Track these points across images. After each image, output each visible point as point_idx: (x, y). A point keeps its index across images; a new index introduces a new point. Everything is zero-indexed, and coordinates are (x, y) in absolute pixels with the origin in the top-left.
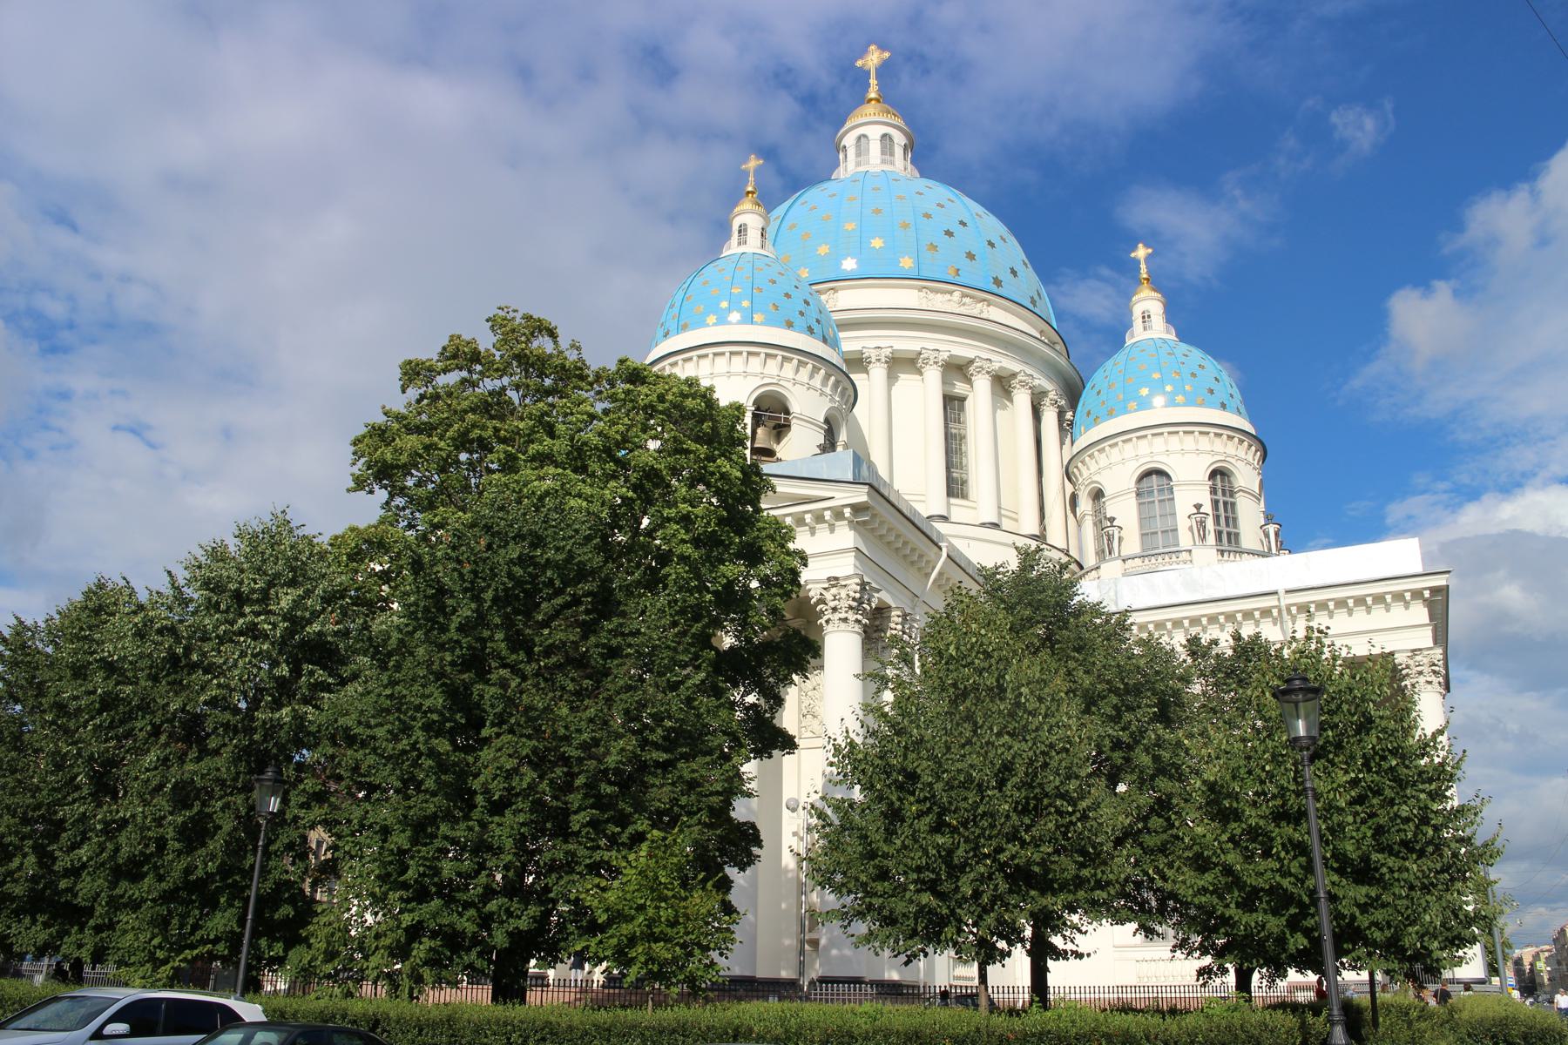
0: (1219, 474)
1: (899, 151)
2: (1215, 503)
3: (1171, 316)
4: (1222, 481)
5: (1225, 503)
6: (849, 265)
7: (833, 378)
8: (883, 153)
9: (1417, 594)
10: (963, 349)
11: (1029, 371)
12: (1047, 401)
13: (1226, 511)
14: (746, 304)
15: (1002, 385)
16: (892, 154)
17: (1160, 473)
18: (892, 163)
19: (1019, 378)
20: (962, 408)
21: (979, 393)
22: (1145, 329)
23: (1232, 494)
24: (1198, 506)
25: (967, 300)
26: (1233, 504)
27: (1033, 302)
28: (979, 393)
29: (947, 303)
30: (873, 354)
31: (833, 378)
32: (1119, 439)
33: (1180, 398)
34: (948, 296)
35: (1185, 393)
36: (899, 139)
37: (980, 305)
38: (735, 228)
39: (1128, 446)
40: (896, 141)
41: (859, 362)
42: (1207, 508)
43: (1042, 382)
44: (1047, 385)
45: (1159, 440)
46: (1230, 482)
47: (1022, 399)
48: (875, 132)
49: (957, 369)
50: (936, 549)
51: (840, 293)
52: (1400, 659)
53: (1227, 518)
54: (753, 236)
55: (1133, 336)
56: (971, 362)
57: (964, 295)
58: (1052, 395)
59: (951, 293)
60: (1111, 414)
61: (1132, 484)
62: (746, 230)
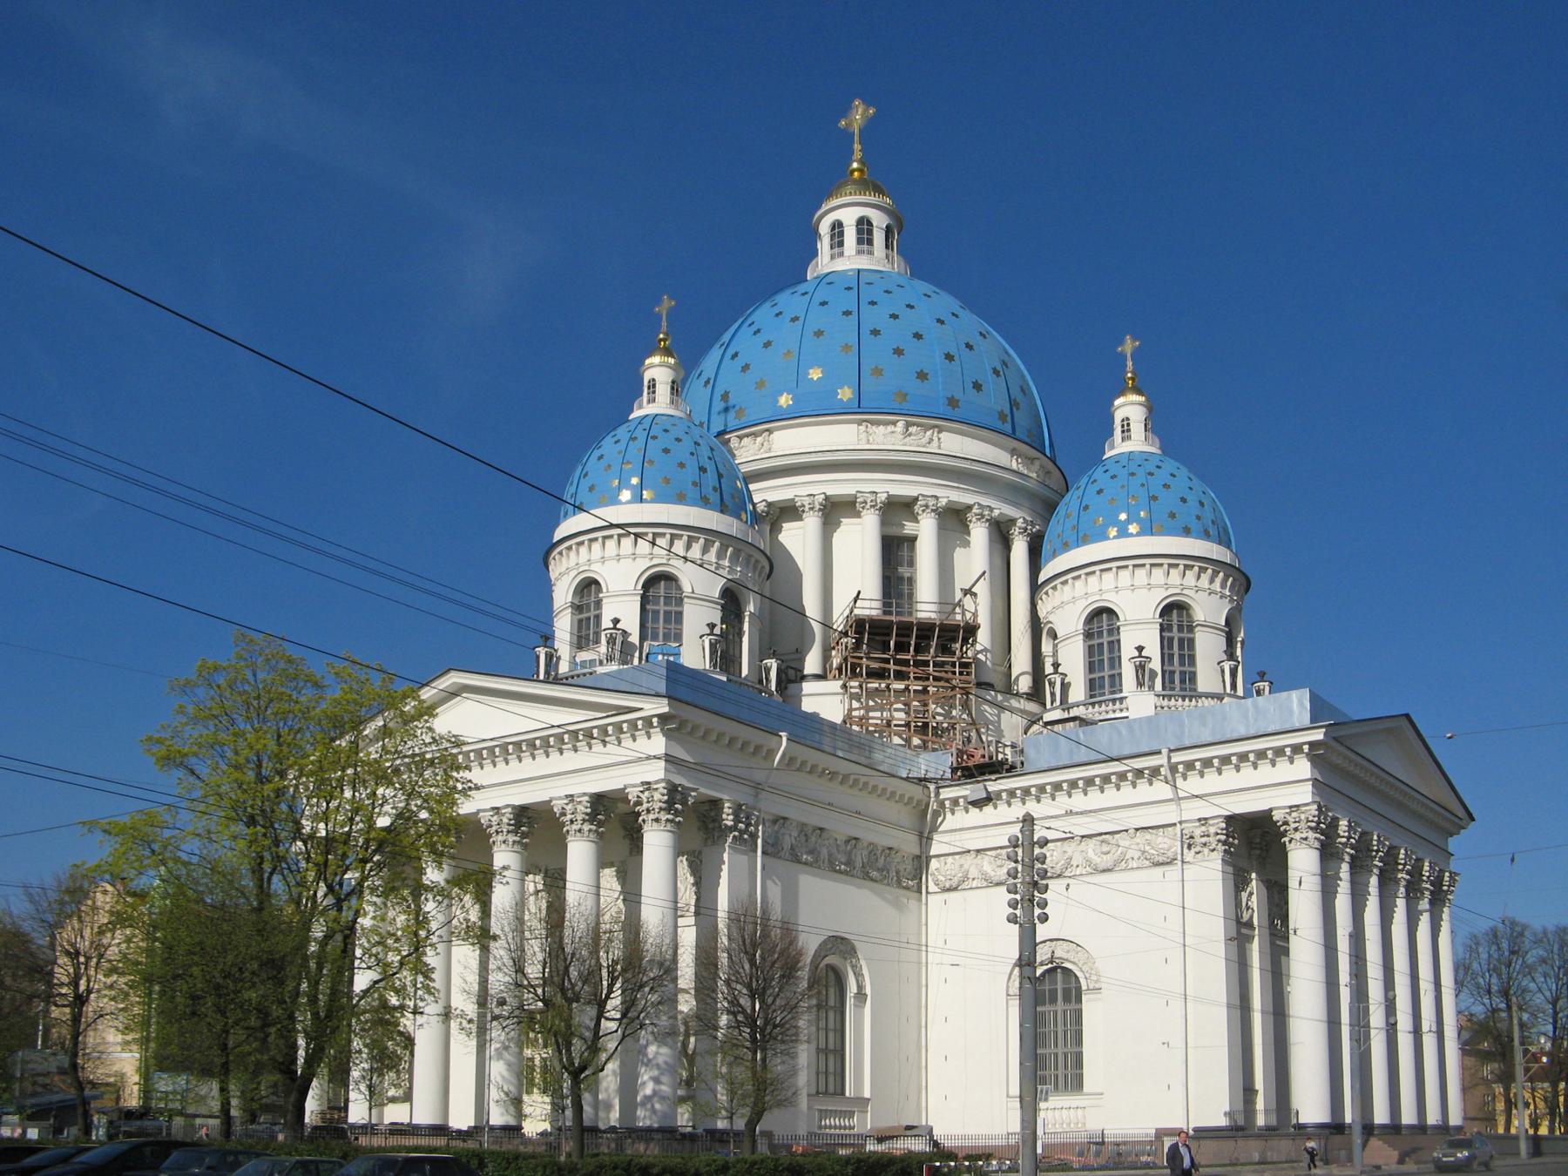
0: (1174, 613)
1: (879, 237)
2: (1165, 643)
3: (1154, 424)
4: (1180, 615)
5: (1181, 641)
6: (784, 400)
7: (730, 549)
8: (860, 241)
9: (1297, 749)
10: (904, 486)
11: (985, 501)
12: (1015, 531)
13: (1181, 647)
14: (635, 481)
15: (954, 520)
16: (870, 242)
17: (1110, 612)
18: (871, 253)
19: (975, 510)
20: (912, 548)
21: (925, 530)
22: (1123, 439)
23: (1191, 629)
24: (1140, 649)
25: (913, 429)
26: (1191, 642)
27: (1002, 416)
28: (925, 530)
29: (888, 438)
30: (807, 501)
31: (730, 549)
32: (1082, 572)
33: (1133, 529)
34: (890, 428)
35: (1139, 521)
36: (879, 220)
37: (929, 433)
38: (646, 383)
39: (1078, 583)
40: (875, 224)
41: (789, 511)
42: (1153, 651)
43: (1002, 509)
44: (1009, 511)
45: (1108, 577)
46: (1189, 616)
47: (979, 534)
48: (849, 217)
49: (897, 509)
50: (776, 738)
51: (776, 434)
52: (1278, 816)
53: (1181, 657)
54: (663, 391)
55: (1112, 447)
56: (916, 499)
57: (908, 425)
58: (1020, 523)
59: (894, 423)
60: (1083, 540)
61: (1080, 626)
62: (654, 386)
